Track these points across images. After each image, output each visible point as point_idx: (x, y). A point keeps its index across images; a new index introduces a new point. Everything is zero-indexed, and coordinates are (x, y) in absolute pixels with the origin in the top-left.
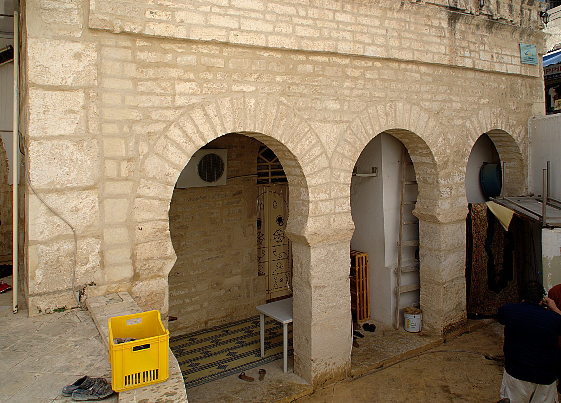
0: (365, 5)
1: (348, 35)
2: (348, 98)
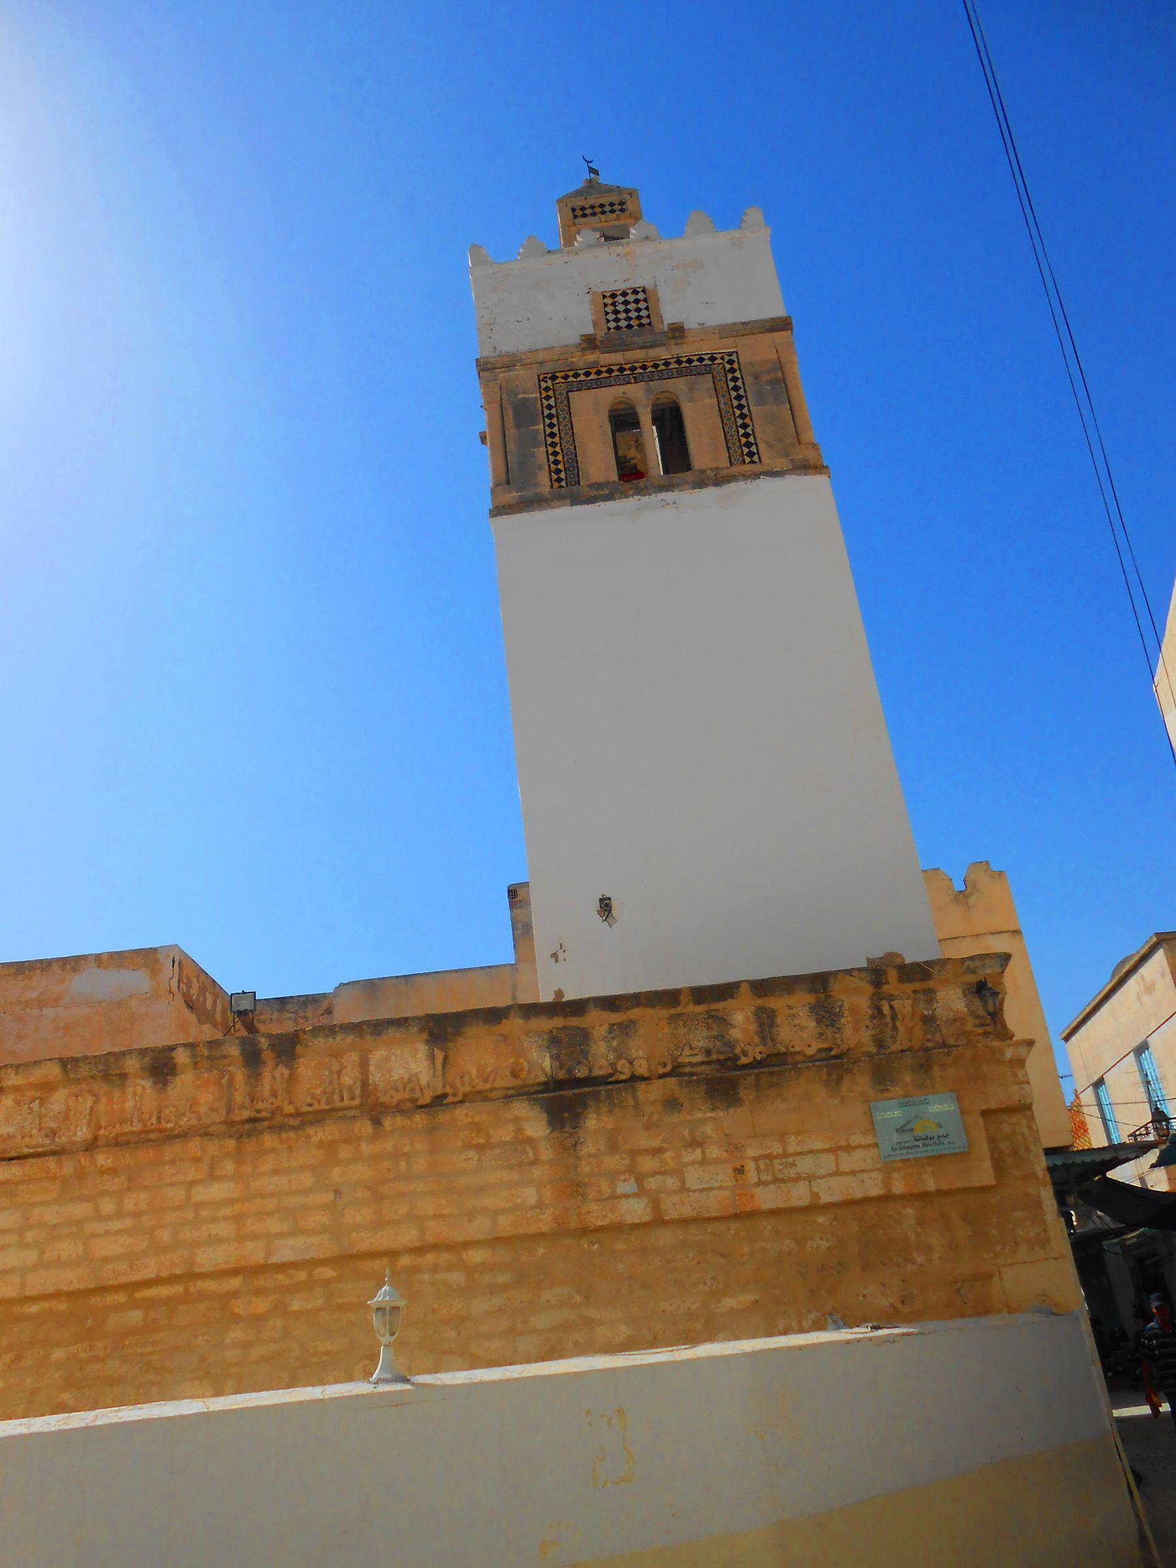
0: (273, 1150)
1: (223, 1229)
2: (236, 1370)
